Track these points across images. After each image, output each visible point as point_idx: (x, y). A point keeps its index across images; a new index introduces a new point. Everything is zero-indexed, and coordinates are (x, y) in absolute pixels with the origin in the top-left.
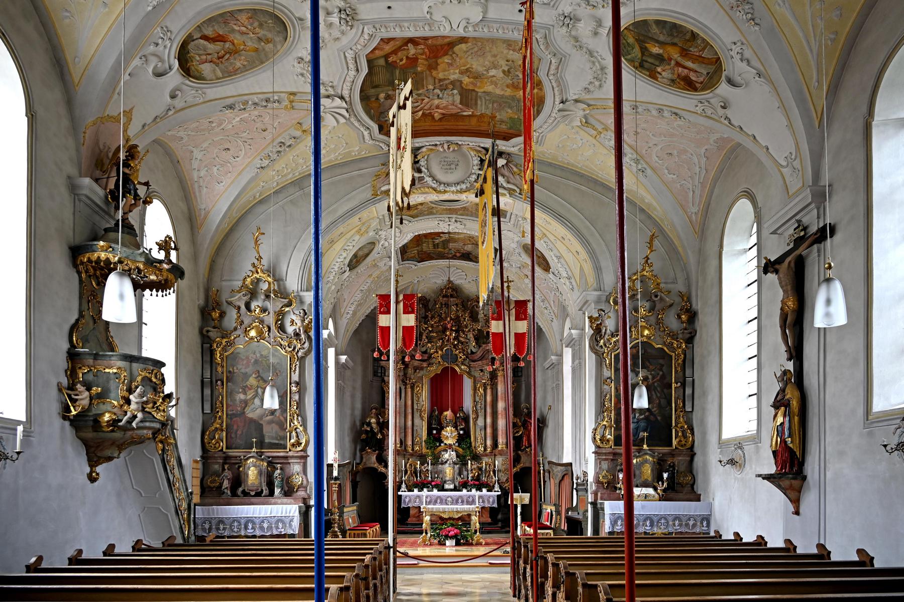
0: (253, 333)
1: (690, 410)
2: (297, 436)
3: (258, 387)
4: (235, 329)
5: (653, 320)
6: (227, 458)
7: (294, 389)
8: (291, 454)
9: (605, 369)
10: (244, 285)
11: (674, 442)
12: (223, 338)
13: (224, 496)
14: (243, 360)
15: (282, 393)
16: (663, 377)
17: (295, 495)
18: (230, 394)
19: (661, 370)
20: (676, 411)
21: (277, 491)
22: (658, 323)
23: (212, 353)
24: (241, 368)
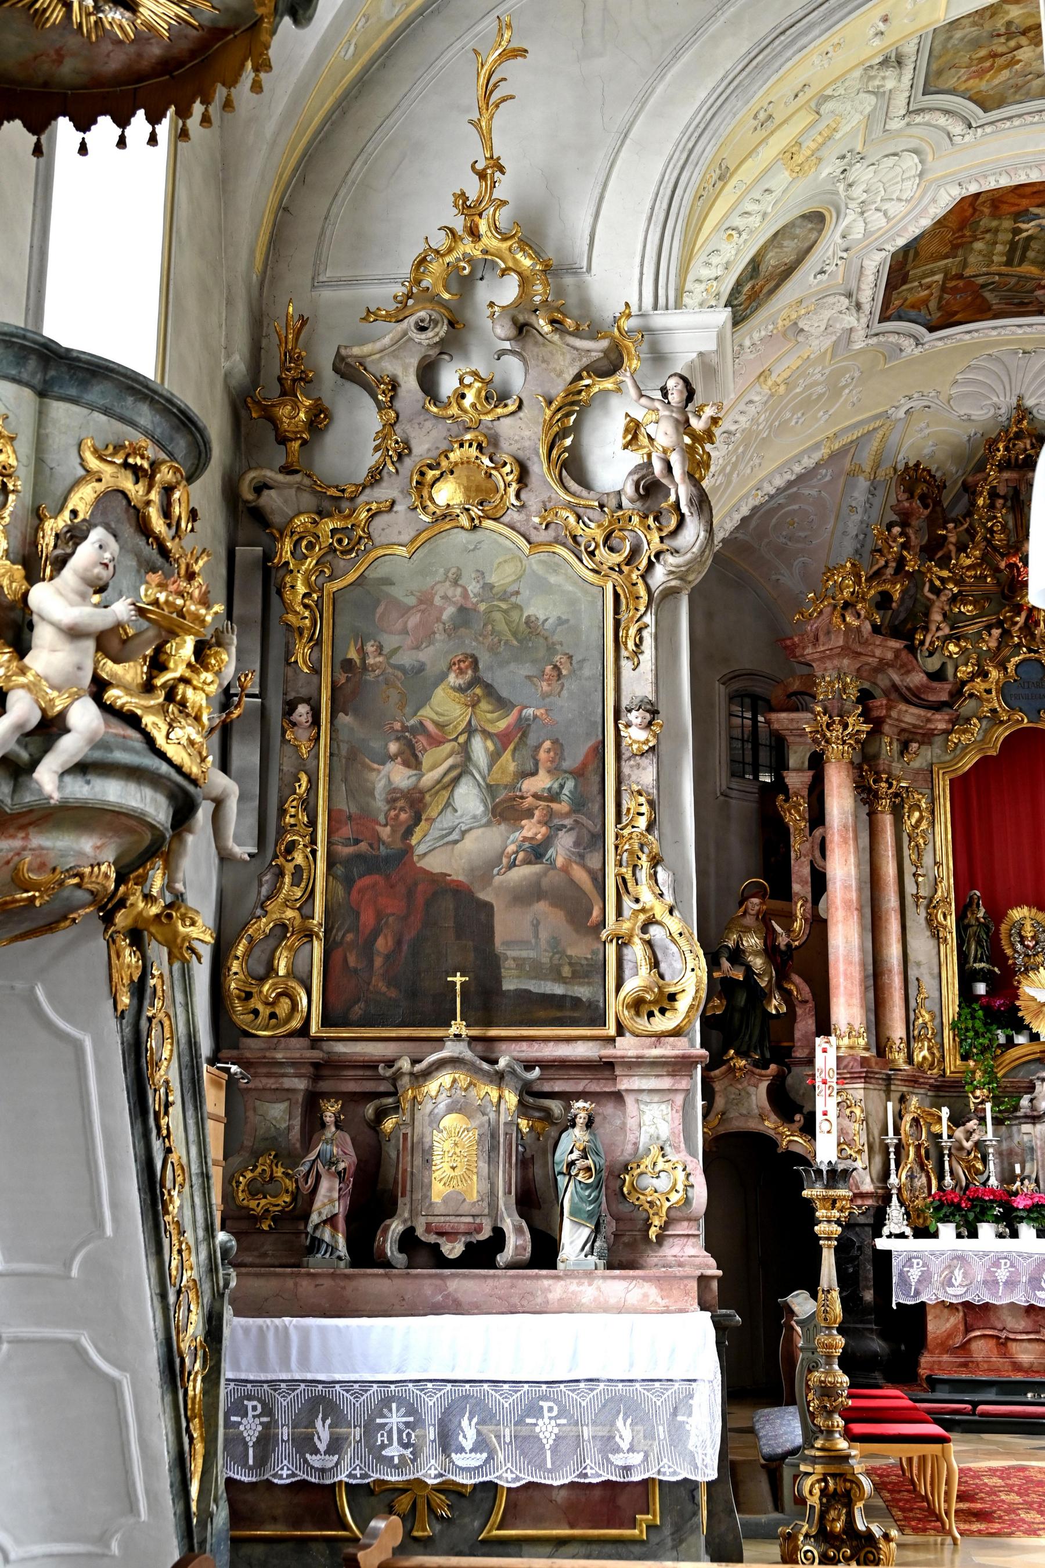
0: (447, 493)
2: (655, 964)
3: (470, 730)
4: (376, 477)
6: (324, 1068)
7: (636, 735)
8: (627, 1047)
10: (415, 293)
12: (322, 513)
13: (317, 1262)
14: (407, 610)
15: (576, 755)
17: (653, 1258)
18: (349, 763)
21: (573, 1238)
23: (271, 578)
24: (397, 646)
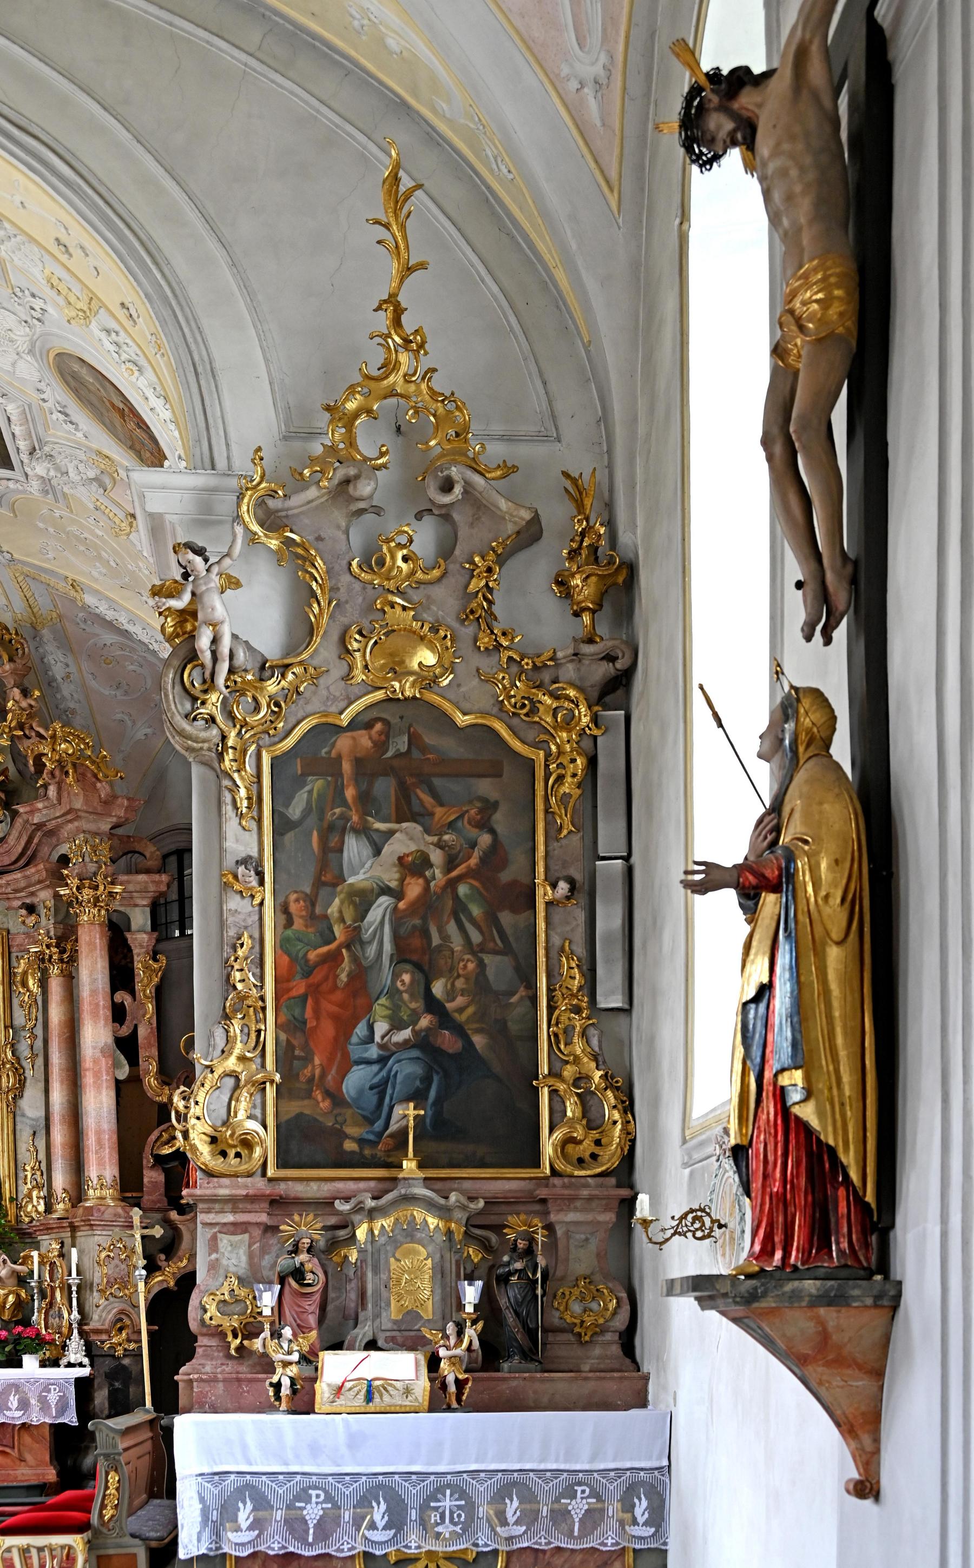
1: (617, 1002)
5: (445, 601)
9: (231, 825)
11: (548, 1148)
16: (495, 857)
19: (484, 824)
20: (551, 1009)
22: (467, 615)
